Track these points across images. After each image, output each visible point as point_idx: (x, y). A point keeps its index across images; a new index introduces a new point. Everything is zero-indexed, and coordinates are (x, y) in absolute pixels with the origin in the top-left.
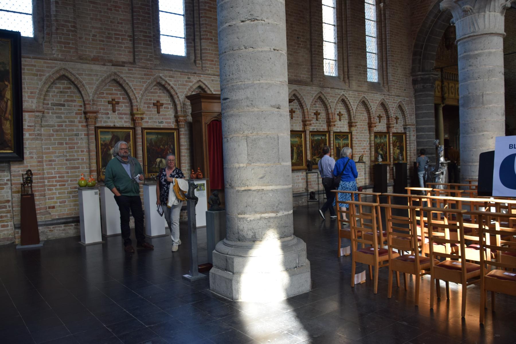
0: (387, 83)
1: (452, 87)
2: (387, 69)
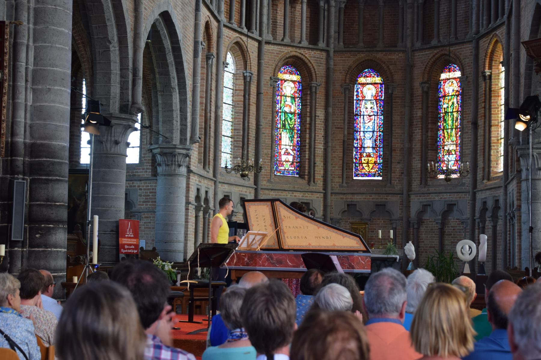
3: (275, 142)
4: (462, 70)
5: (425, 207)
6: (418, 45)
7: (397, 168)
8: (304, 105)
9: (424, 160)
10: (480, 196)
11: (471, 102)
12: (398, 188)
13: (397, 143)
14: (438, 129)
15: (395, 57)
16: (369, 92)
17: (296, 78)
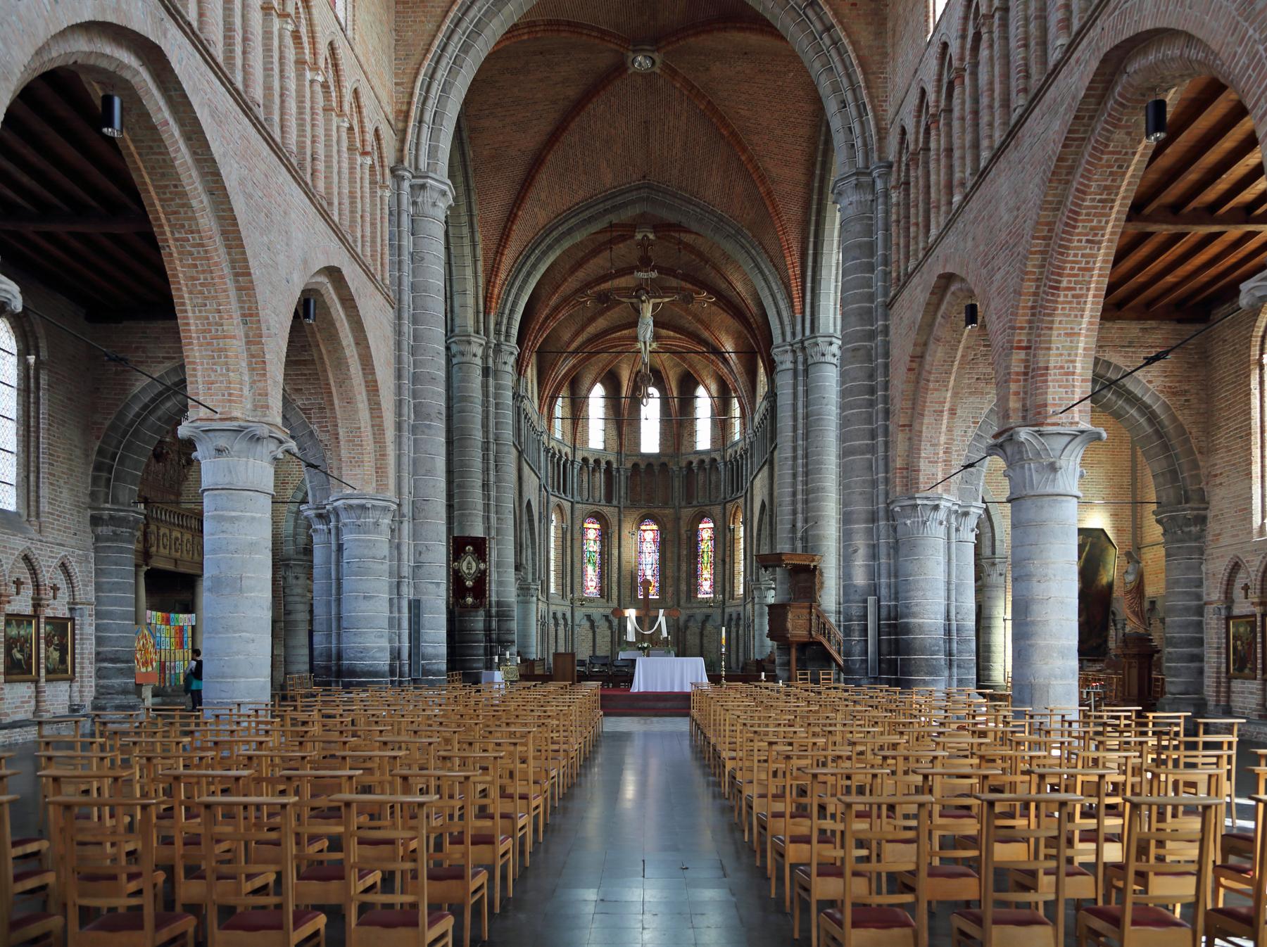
0: (38, 515)
1: (164, 535)
2: (38, 487)
3: (583, 573)
4: (714, 522)
5: (690, 617)
6: (683, 504)
7: (670, 590)
8: (602, 545)
9: (688, 584)
10: (727, 610)
11: (721, 546)
12: (670, 604)
13: (669, 573)
14: (697, 563)
15: (667, 512)
16: (649, 536)
17: (597, 526)
